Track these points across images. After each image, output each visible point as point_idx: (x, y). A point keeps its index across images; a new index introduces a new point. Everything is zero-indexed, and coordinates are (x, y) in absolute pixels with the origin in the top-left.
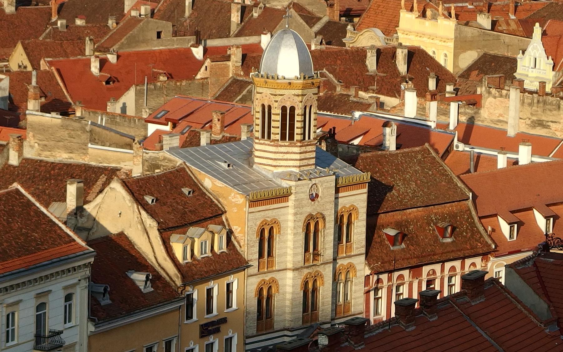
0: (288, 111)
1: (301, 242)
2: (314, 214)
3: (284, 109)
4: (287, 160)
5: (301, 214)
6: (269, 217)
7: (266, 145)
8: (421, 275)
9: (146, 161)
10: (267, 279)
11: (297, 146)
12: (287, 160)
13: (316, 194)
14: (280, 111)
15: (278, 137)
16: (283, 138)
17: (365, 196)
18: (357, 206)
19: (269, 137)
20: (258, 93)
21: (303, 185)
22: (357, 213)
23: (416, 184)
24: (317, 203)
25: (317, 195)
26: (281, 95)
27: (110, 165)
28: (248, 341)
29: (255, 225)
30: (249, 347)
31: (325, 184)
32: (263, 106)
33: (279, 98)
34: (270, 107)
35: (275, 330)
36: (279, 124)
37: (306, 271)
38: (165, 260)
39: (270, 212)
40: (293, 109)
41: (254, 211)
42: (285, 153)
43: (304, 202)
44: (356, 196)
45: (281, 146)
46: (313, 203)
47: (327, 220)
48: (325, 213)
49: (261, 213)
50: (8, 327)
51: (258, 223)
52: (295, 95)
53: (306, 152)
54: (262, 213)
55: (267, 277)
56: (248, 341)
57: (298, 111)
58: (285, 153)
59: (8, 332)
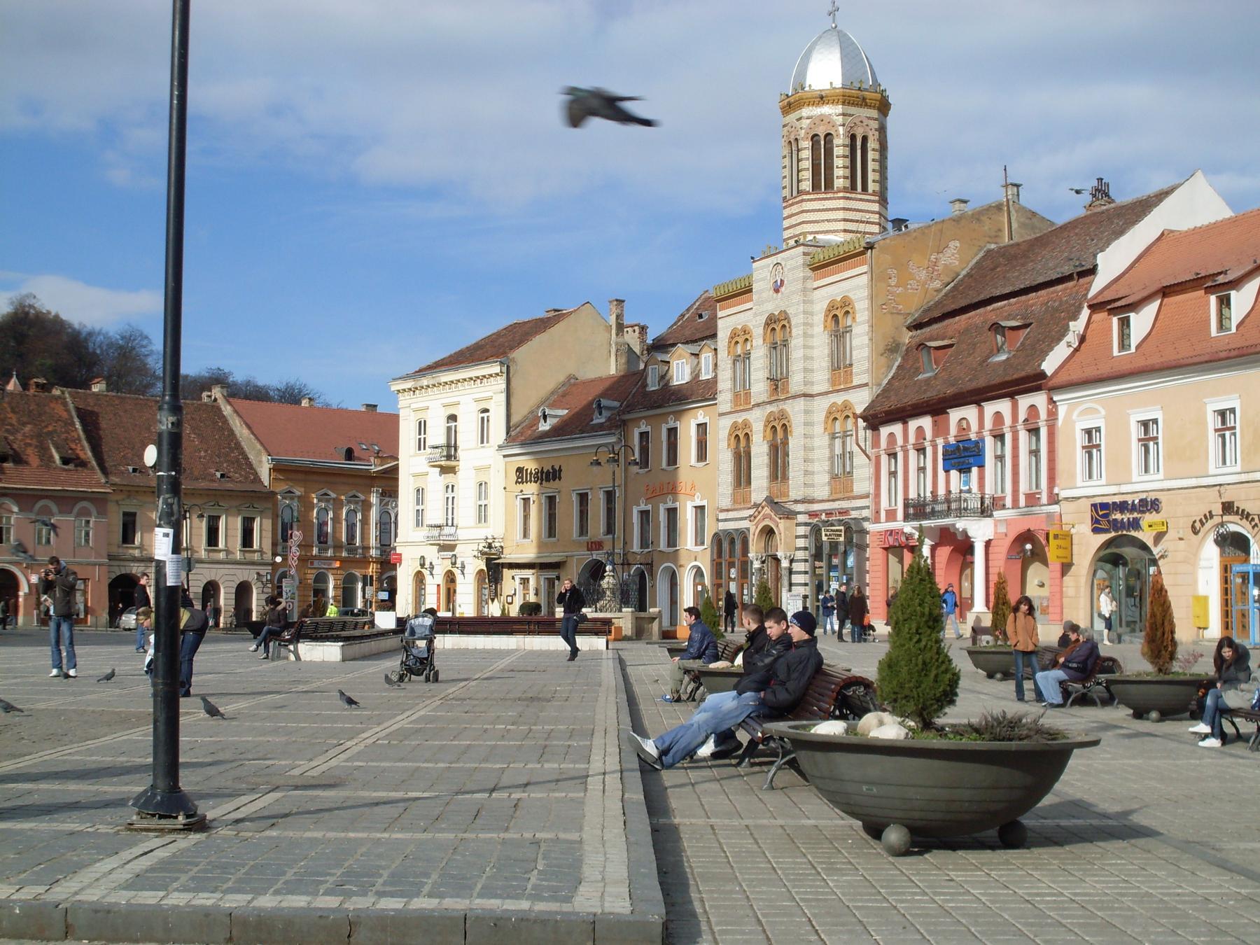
2: (776, 313)
5: (761, 314)
10: (740, 421)
17: (865, 279)
21: (762, 268)
28: (722, 516)
30: (722, 526)
31: (790, 262)
37: (770, 409)
46: (775, 295)
50: (420, 434)
56: (722, 516)
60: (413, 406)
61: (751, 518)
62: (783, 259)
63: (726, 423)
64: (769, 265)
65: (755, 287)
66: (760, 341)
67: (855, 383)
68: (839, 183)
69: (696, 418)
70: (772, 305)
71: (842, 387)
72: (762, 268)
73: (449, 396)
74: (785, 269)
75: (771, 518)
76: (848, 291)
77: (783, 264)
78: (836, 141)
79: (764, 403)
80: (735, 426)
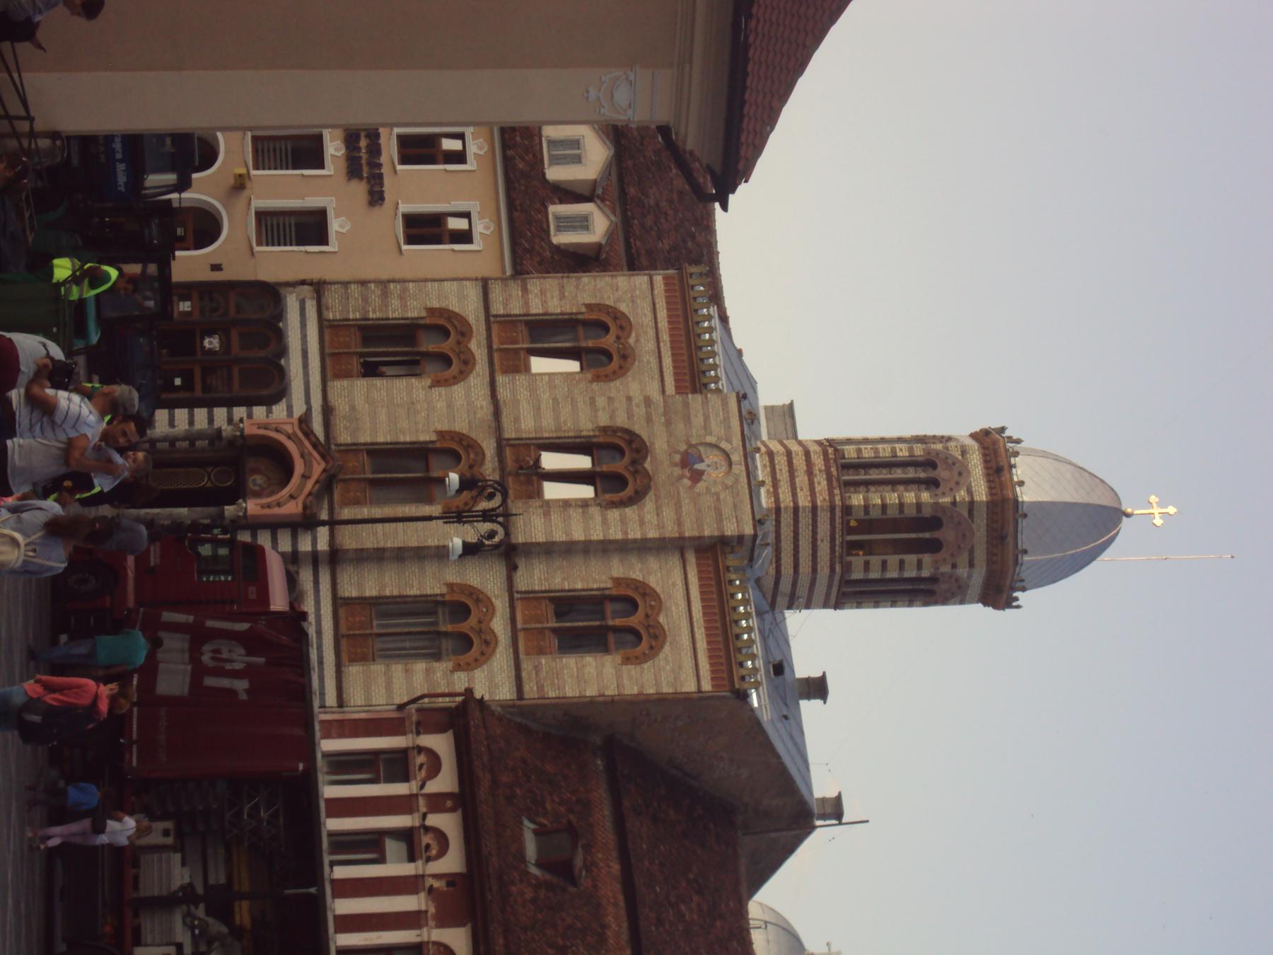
2: (647, 465)
5: (649, 420)
6: (637, 341)
8: (442, 922)
10: (473, 345)
13: (701, 473)
17: (690, 687)
18: (661, 655)
24: (677, 471)
29: (619, 300)
31: (730, 500)
35: (329, 384)
37: (489, 447)
39: (651, 345)
41: (656, 292)
43: (681, 426)
44: (690, 654)
46: (677, 458)
47: (630, 512)
48: (649, 504)
49: (650, 315)
51: (623, 307)
53: (810, 472)
54: (647, 319)
55: (477, 347)
61: (305, 421)
62: (737, 481)
63: (467, 304)
64: (729, 440)
65: (695, 400)
67: (527, 665)
68: (858, 561)
75: (305, 477)
78: (927, 558)
79: (499, 429)
80: (465, 331)
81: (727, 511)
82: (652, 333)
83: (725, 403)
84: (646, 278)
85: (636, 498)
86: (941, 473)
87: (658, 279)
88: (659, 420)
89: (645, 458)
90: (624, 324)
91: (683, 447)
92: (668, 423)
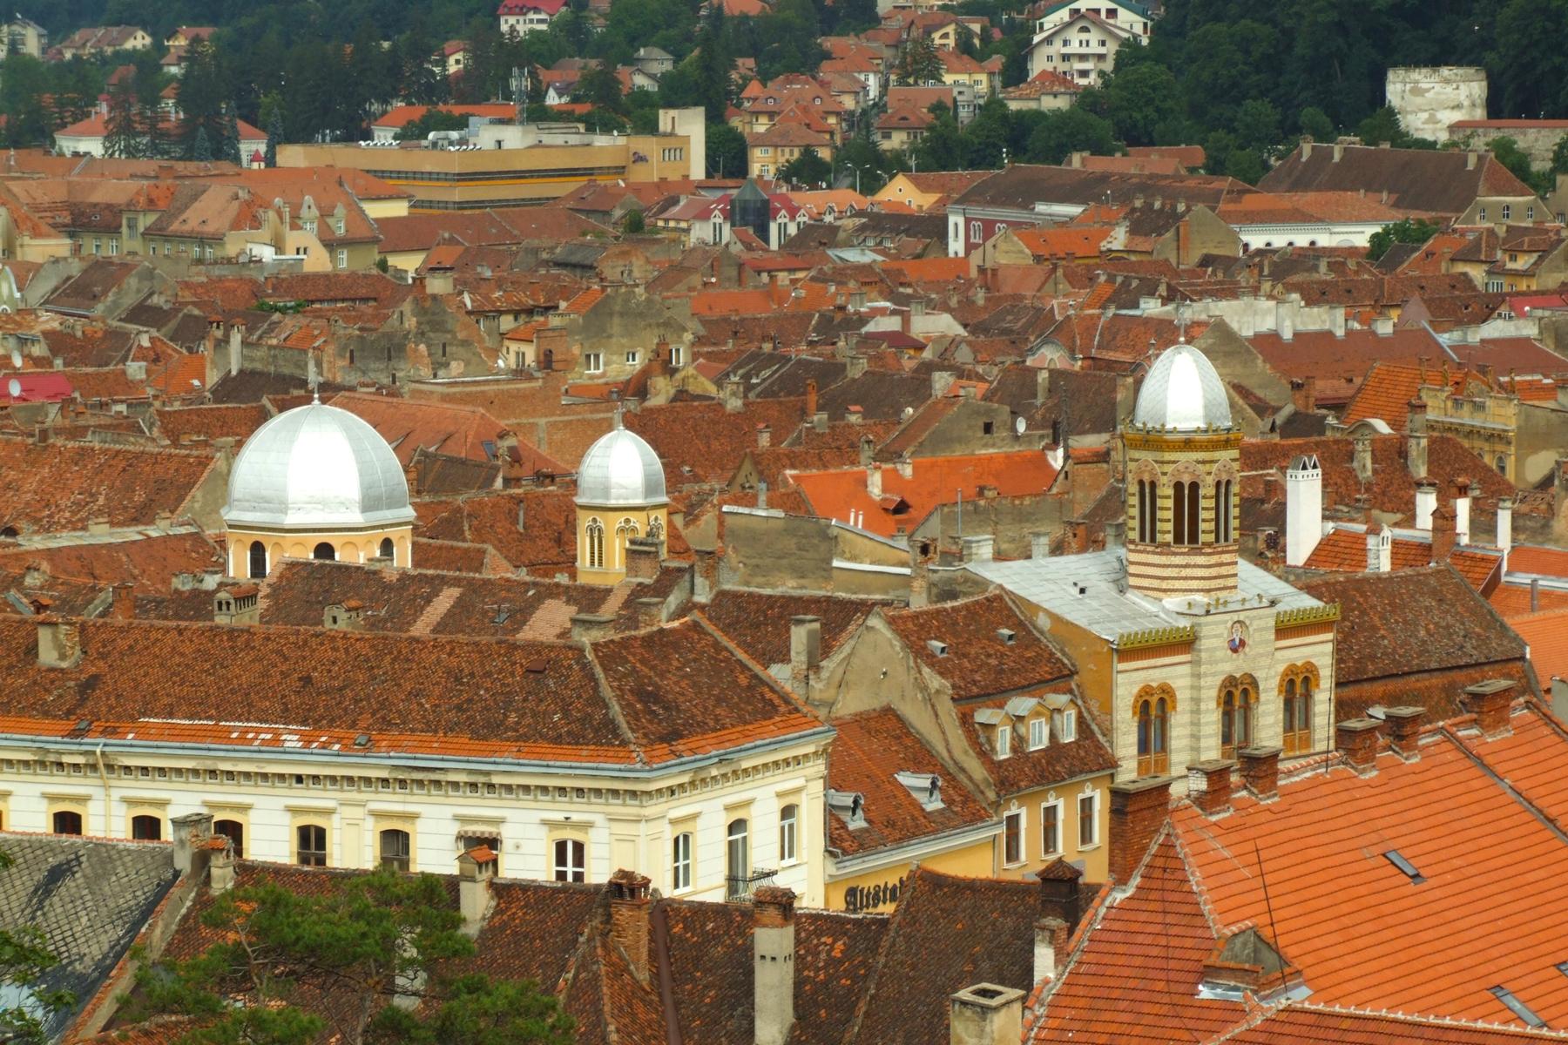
0: (1186, 492)
1: (1214, 727)
2: (1238, 676)
3: (1178, 486)
4: (1185, 578)
5: (1214, 674)
7: (1148, 552)
9: (934, 585)
11: (1204, 554)
12: (1185, 578)
14: (1170, 492)
15: (1170, 538)
16: (1178, 539)
17: (1329, 647)
19: (1153, 539)
20: (1132, 460)
21: (1216, 623)
22: (1317, 677)
23: (1428, 631)
24: (1242, 655)
25: (1242, 643)
26: (1174, 462)
27: (871, 597)
32: (1141, 483)
33: (1169, 468)
34: (1153, 485)
36: (1170, 515)
38: (966, 752)
39: (1157, 671)
40: (1194, 487)
42: (1182, 566)
45: (1175, 554)
46: (1235, 655)
47: (1261, 688)
48: (1257, 674)
49: (1140, 672)
50: (676, 859)
51: (1135, 690)
52: (1198, 462)
57: (1207, 490)
58: (1182, 566)
59: (677, 869)
60: (675, 814)
64: (1226, 622)
66: (1213, 705)
69: (1084, 792)
70: (1234, 666)
71: (1298, 753)
72: (1216, 623)
73: (735, 792)
74: (1251, 629)
76: (1315, 656)
77: (1248, 623)
81: (1262, 623)
82: (1151, 671)
83: (1207, 624)
84: (1120, 676)
85: (1254, 683)
86: (1224, 478)
87: (1122, 666)
88: (1213, 669)
89: (1235, 678)
90: (1147, 690)
91: (1229, 652)
92: (1216, 662)
